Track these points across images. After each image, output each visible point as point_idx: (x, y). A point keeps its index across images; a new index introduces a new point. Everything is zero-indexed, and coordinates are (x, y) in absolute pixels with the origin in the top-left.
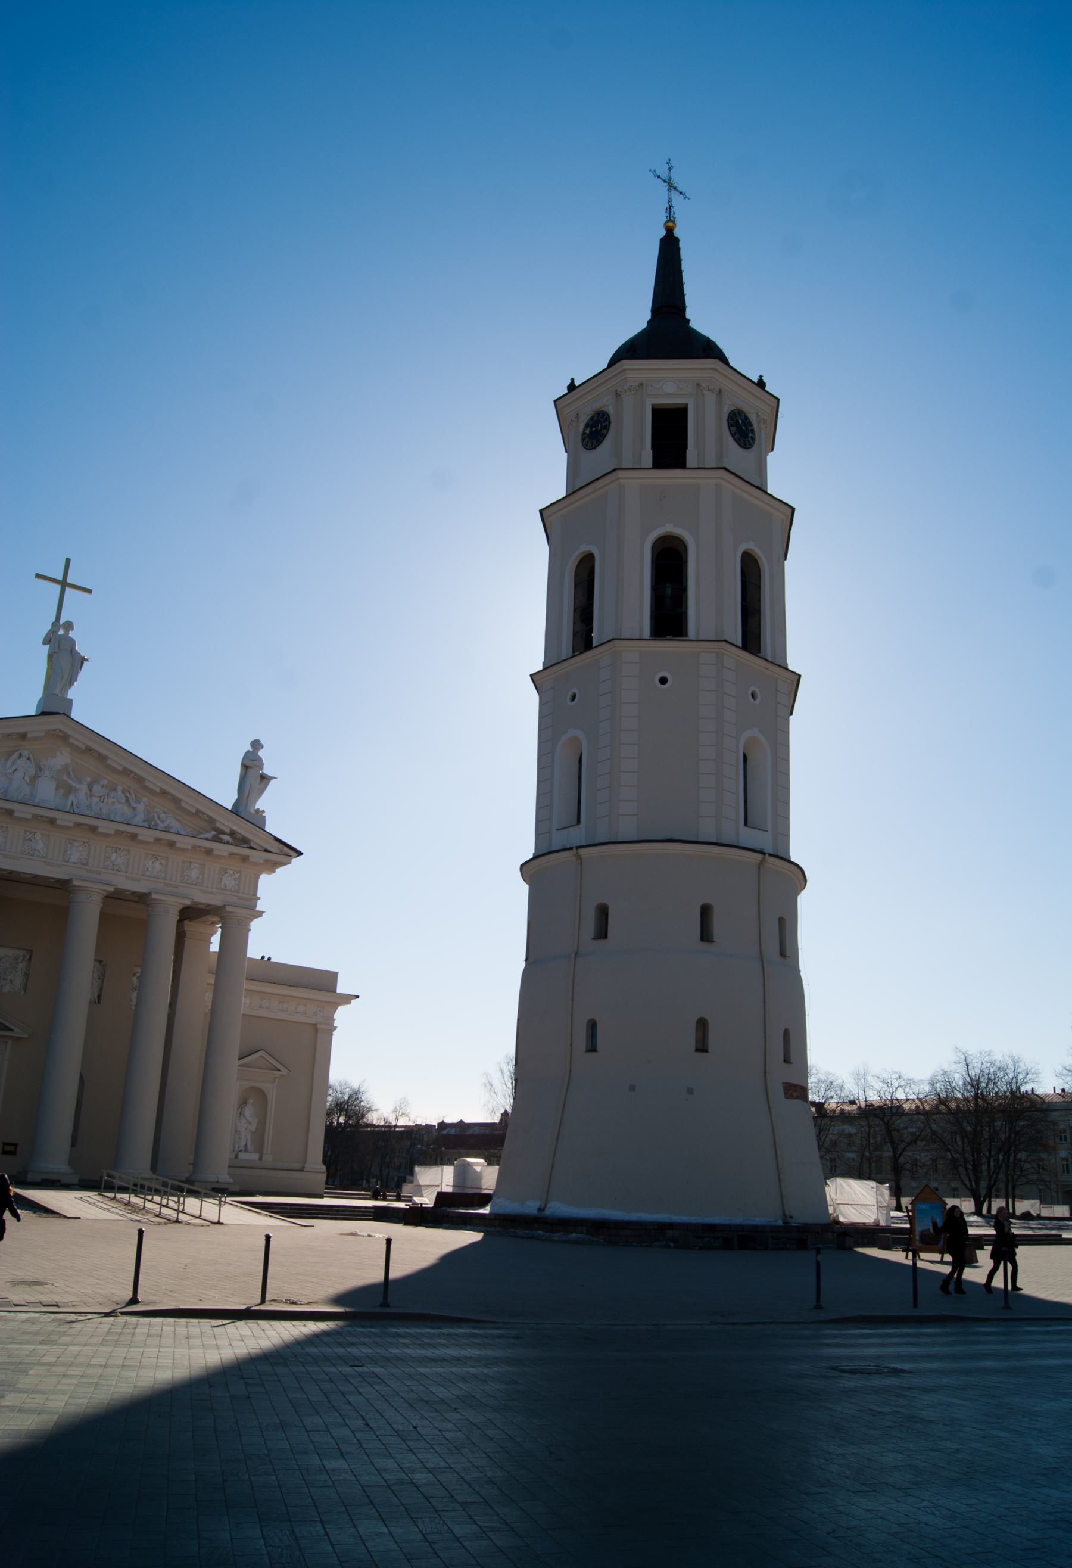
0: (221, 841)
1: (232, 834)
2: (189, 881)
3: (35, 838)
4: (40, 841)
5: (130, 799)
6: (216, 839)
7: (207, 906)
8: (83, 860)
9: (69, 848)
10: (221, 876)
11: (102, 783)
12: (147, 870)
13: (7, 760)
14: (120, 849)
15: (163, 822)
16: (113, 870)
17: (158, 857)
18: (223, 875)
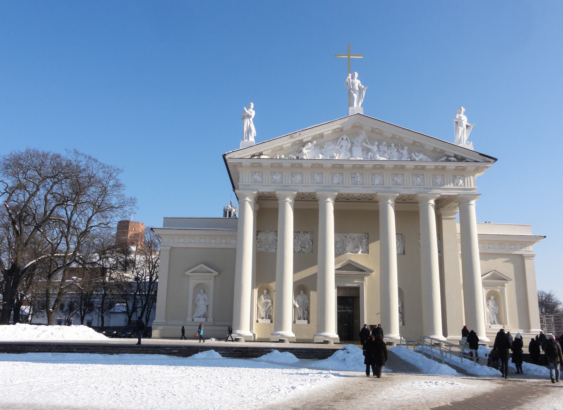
0: (450, 161)
1: (455, 156)
2: (437, 185)
3: (356, 176)
4: (359, 177)
5: (399, 149)
6: (448, 160)
7: (449, 197)
8: (381, 183)
9: (373, 178)
10: (453, 179)
11: (383, 144)
12: (414, 183)
13: (337, 142)
14: (398, 174)
15: (417, 157)
16: (397, 185)
17: (418, 175)
18: (454, 179)
